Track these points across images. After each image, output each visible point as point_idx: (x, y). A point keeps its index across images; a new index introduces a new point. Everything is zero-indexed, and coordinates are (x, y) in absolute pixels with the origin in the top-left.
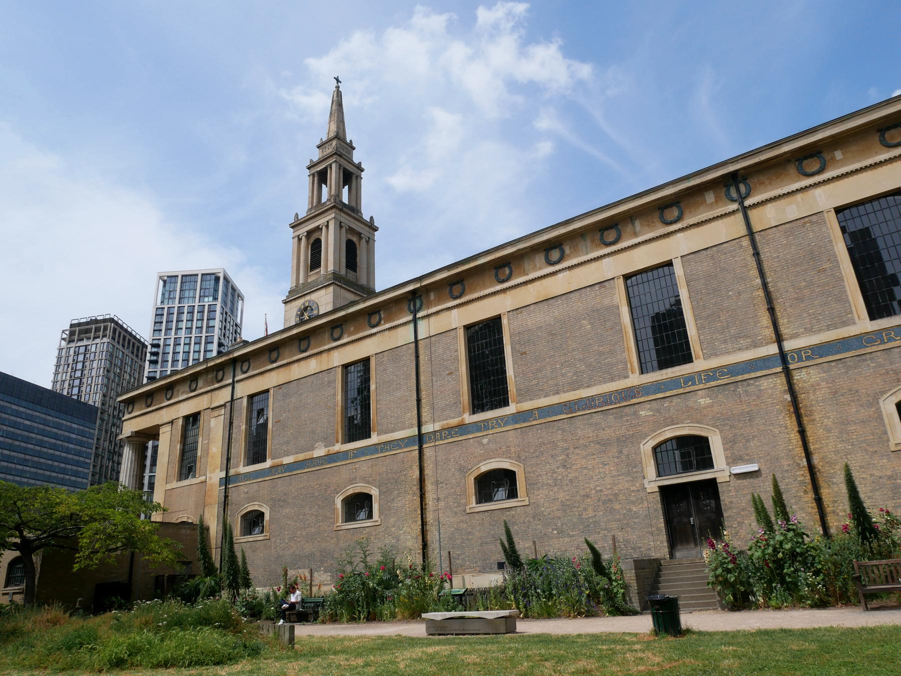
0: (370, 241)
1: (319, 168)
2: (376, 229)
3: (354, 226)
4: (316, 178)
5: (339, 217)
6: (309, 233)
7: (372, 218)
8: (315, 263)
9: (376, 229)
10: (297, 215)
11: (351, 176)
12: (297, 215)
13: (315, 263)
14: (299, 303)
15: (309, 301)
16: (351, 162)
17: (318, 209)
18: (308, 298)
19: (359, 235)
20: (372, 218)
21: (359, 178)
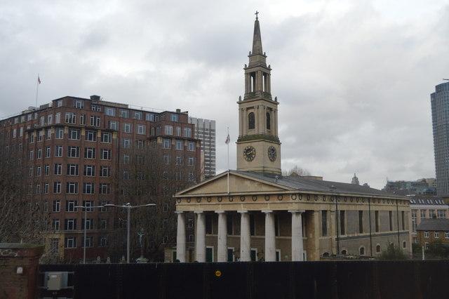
1: (252, 70)
2: (278, 103)
3: (269, 106)
5: (264, 105)
6: (248, 109)
7: (276, 98)
8: (252, 125)
9: (278, 103)
10: (240, 97)
11: (267, 75)
12: (240, 97)
13: (252, 125)
14: (246, 145)
16: (266, 68)
17: (250, 96)
18: (249, 144)
19: (271, 109)
20: (276, 98)
21: (269, 75)
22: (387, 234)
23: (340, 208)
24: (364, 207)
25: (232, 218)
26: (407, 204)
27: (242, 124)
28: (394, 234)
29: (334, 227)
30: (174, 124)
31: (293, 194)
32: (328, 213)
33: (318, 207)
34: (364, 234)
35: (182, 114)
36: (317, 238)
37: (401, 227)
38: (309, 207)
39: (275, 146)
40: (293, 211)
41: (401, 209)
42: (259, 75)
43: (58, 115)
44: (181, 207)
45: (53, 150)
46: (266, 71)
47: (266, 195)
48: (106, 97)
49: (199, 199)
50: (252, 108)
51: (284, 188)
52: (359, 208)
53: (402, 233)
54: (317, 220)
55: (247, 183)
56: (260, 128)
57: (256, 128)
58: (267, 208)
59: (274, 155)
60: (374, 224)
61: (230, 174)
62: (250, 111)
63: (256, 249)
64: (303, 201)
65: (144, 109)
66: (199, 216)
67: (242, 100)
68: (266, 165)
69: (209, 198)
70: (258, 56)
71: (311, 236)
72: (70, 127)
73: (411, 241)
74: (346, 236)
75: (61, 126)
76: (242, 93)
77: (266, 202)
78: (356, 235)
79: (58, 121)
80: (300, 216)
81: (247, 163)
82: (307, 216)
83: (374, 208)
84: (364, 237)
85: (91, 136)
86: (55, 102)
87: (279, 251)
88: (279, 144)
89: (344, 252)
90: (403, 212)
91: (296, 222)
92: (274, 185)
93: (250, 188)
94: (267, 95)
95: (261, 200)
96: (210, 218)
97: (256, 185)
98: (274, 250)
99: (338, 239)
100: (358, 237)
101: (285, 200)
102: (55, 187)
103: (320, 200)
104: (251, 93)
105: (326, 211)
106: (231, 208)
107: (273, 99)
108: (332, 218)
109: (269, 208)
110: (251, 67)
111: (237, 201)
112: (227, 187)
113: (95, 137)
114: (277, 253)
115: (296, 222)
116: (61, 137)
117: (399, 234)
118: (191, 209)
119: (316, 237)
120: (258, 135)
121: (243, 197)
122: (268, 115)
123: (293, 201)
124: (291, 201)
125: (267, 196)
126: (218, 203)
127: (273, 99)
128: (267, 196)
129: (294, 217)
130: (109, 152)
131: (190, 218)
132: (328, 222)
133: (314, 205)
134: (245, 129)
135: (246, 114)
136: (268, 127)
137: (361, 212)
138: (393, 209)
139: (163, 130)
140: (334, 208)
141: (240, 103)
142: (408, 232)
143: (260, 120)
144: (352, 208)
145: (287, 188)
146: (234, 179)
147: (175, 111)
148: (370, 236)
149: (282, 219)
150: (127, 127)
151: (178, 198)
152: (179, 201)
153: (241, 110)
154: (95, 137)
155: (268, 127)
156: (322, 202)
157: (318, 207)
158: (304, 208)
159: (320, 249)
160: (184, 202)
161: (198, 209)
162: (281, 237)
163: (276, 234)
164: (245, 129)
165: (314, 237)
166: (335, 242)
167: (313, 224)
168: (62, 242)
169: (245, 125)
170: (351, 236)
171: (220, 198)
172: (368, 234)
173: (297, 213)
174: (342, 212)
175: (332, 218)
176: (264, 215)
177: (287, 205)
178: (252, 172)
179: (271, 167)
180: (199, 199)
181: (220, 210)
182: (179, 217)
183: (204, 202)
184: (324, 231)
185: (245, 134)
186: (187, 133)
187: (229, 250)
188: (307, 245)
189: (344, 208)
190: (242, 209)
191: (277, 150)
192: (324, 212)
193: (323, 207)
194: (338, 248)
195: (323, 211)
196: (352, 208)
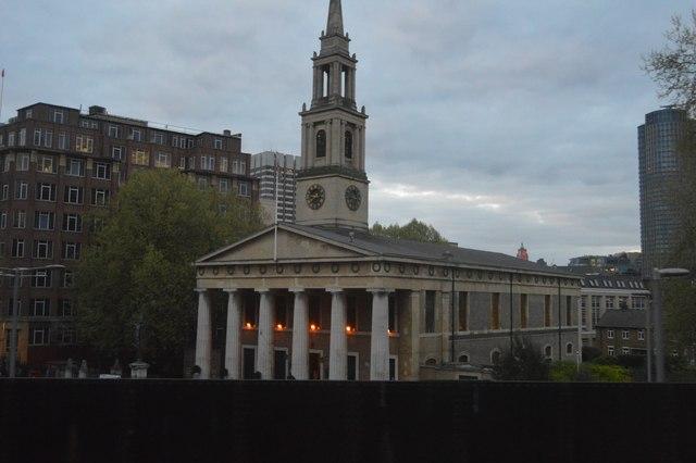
0: (362, 128)
1: (326, 61)
4: (320, 71)
6: (316, 124)
8: (321, 151)
13: (321, 151)
16: (346, 56)
17: (321, 103)
18: (316, 182)
19: (353, 126)
21: (354, 69)
22: (542, 332)
23: (459, 287)
24: (502, 288)
25: (282, 302)
26: (576, 286)
27: (307, 148)
28: (554, 331)
29: (446, 317)
30: (217, 154)
31: (375, 263)
32: (438, 295)
33: (419, 285)
34: (501, 330)
35: (231, 137)
36: (417, 336)
37: (564, 319)
38: (402, 285)
39: (359, 185)
40: (376, 291)
41: (565, 292)
42: (336, 67)
43: (23, 132)
44: (205, 282)
45: (11, 187)
46: (345, 62)
47: (334, 264)
48: (114, 110)
49: (231, 268)
50: (322, 122)
51: (361, 251)
52: (493, 289)
53: (565, 330)
54: (416, 306)
55: (305, 244)
56: (335, 156)
57: (327, 153)
58: (334, 285)
59: (356, 199)
60: (517, 316)
62: (320, 128)
63: (356, 354)
64: (391, 273)
65: (170, 129)
66: (231, 297)
67: (308, 109)
68: (340, 216)
69: (247, 268)
70: (336, 39)
71: (406, 332)
72: (39, 152)
73: (580, 344)
74: (468, 332)
75: (26, 150)
76: (307, 99)
78: (486, 332)
79: (23, 143)
80: (387, 298)
82: (398, 301)
83: (518, 290)
84: (498, 335)
85: (101, 170)
86: (22, 112)
88: (367, 183)
89: (464, 359)
90: (569, 297)
91: (380, 308)
92: (345, 246)
93: (310, 251)
94: (348, 103)
95: (325, 273)
96: (249, 301)
97: (319, 247)
98: (344, 353)
99: (452, 338)
100: (490, 335)
101: (362, 272)
102: (15, 248)
103: (424, 274)
104: (322, 98)
105: (434, 292)
106: (279, 285)
107: (359, 110)
108: (444, 307)
109: (336, 285)
110: (323, 56)
111: (288, 272)
112: (274, 249)
113: (108, 172)
114: (392, 361)
115: (380, 308)
116: (25, 167)
117: (560, 331)
118: (219, 285)
119: (413, 333)
121: (297, 267)
122: (348, 135)
124: (372, 273)
125: (335, 266)
126: (260, 275)
127: (359, 110)
128: (335, 266)
129: (376, 300)
130: (53, 189)
131: (218, 299)
132: (437, 311)
133: (414, 282)
134: (310, 156)
136: (349, 154)
137: (496, 295)
138: (553, 292)
139: (198, 163)
140: (448, 287)
141: (304, 114)
142: (576, 330)
143: (334, 142)
144: (481, 288)
145: (365, 252)
146: (285, 237)
147: (222, 133)
148: (511, 334)
149: (358, 304)
150: (140, 158)
151: (200, 268)
153: (305, 126)
154: (108, 172)
155: (349, 154)
156: (424, 276)
157: (419, 285)
158: (393, 285)
159: (422, 354)
160: (209, 274)
161: (230, 285)
162: (360, 333)
164: (310, 156)
165: (410, 331)
166: (447, 344)
167: (410, 313)
168: (24, 336)
169: (310, 152)
170: (476, 333)
171: (263, 267)
172: (507, 330)
173: (381, 294)
174: (463, 294)
175: (444, 307)
176: (330, 295)
177: (365, 280)
178: (320, 227)
179: (348, 218)
180: (231, 268)
181: (262, 287)
182: (201, 297)
183: (239, 274)
184: (429, 323)
185: (310, 165)
186: (238, 170)
187: (277, 352)
188: (398, 346)
189: (468, 288)
190: (296, 286)
191: (362, 193)
192: (431, 294)
193: (428, 286)
194: (453, 351)
195: (427, 291)
196: (481, 288)
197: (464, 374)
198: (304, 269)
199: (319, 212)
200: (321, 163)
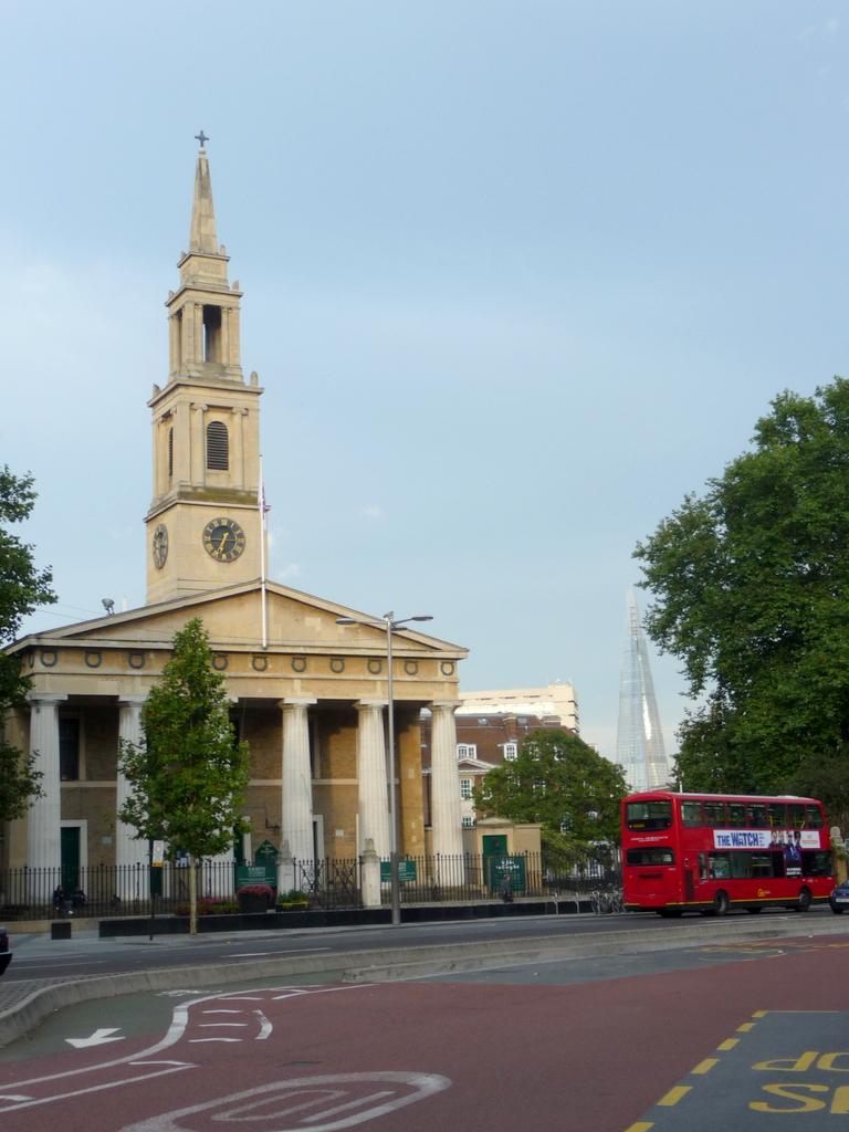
4: (200, 314)
6: (211, 407)
15: (230, 522)
55: (314, 622)
61: (267, 591)
77: (372, 677)
81: (212, 566)
87: (320, 819)
106: (260, 691)
111: (276, 668)
118: (105, 688)
120: (234, 492)
121: (299, 659)
123: (444, 678)
124: (440, 676)
135: (199, 423)
152: (49, 659)
160: (66, 665)
163: (313, 777)
177: (429, 688)
197: (489, 832)
198: (312, 663)
199: (239, 564)
200: (218, 480)
